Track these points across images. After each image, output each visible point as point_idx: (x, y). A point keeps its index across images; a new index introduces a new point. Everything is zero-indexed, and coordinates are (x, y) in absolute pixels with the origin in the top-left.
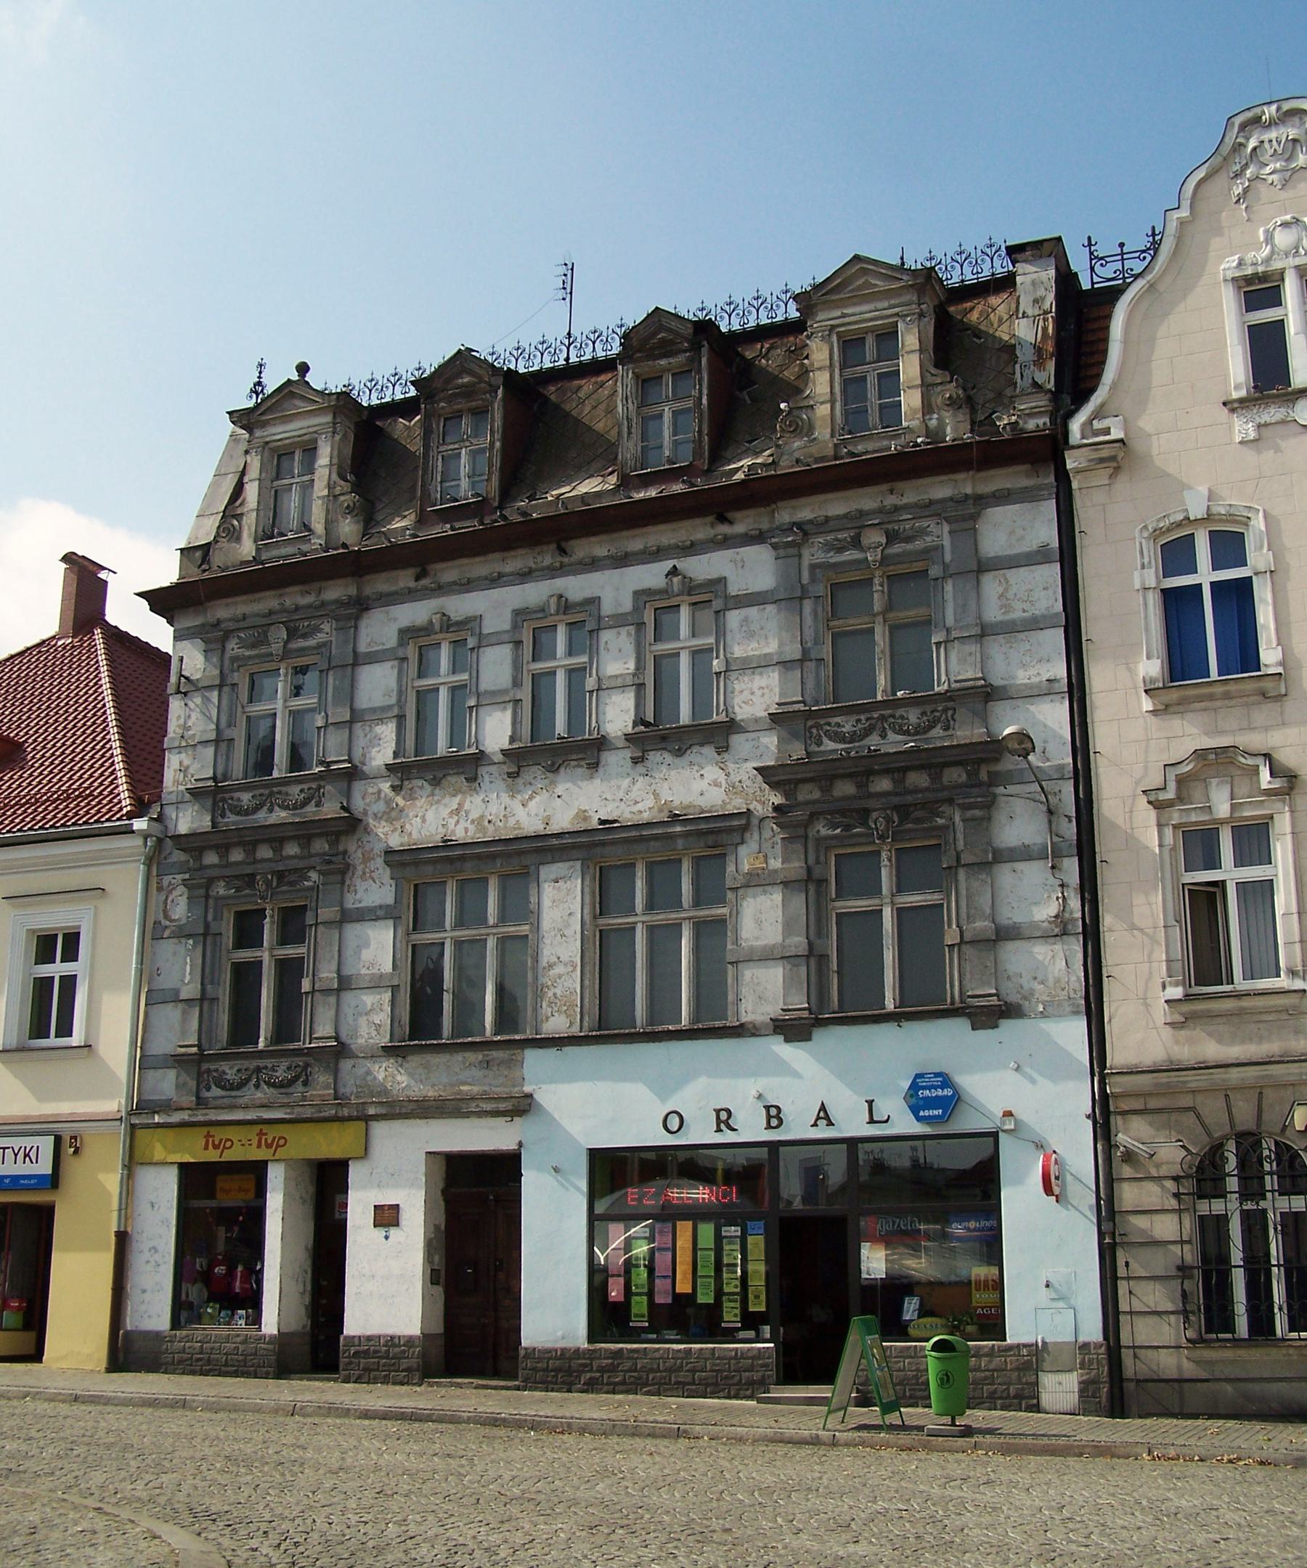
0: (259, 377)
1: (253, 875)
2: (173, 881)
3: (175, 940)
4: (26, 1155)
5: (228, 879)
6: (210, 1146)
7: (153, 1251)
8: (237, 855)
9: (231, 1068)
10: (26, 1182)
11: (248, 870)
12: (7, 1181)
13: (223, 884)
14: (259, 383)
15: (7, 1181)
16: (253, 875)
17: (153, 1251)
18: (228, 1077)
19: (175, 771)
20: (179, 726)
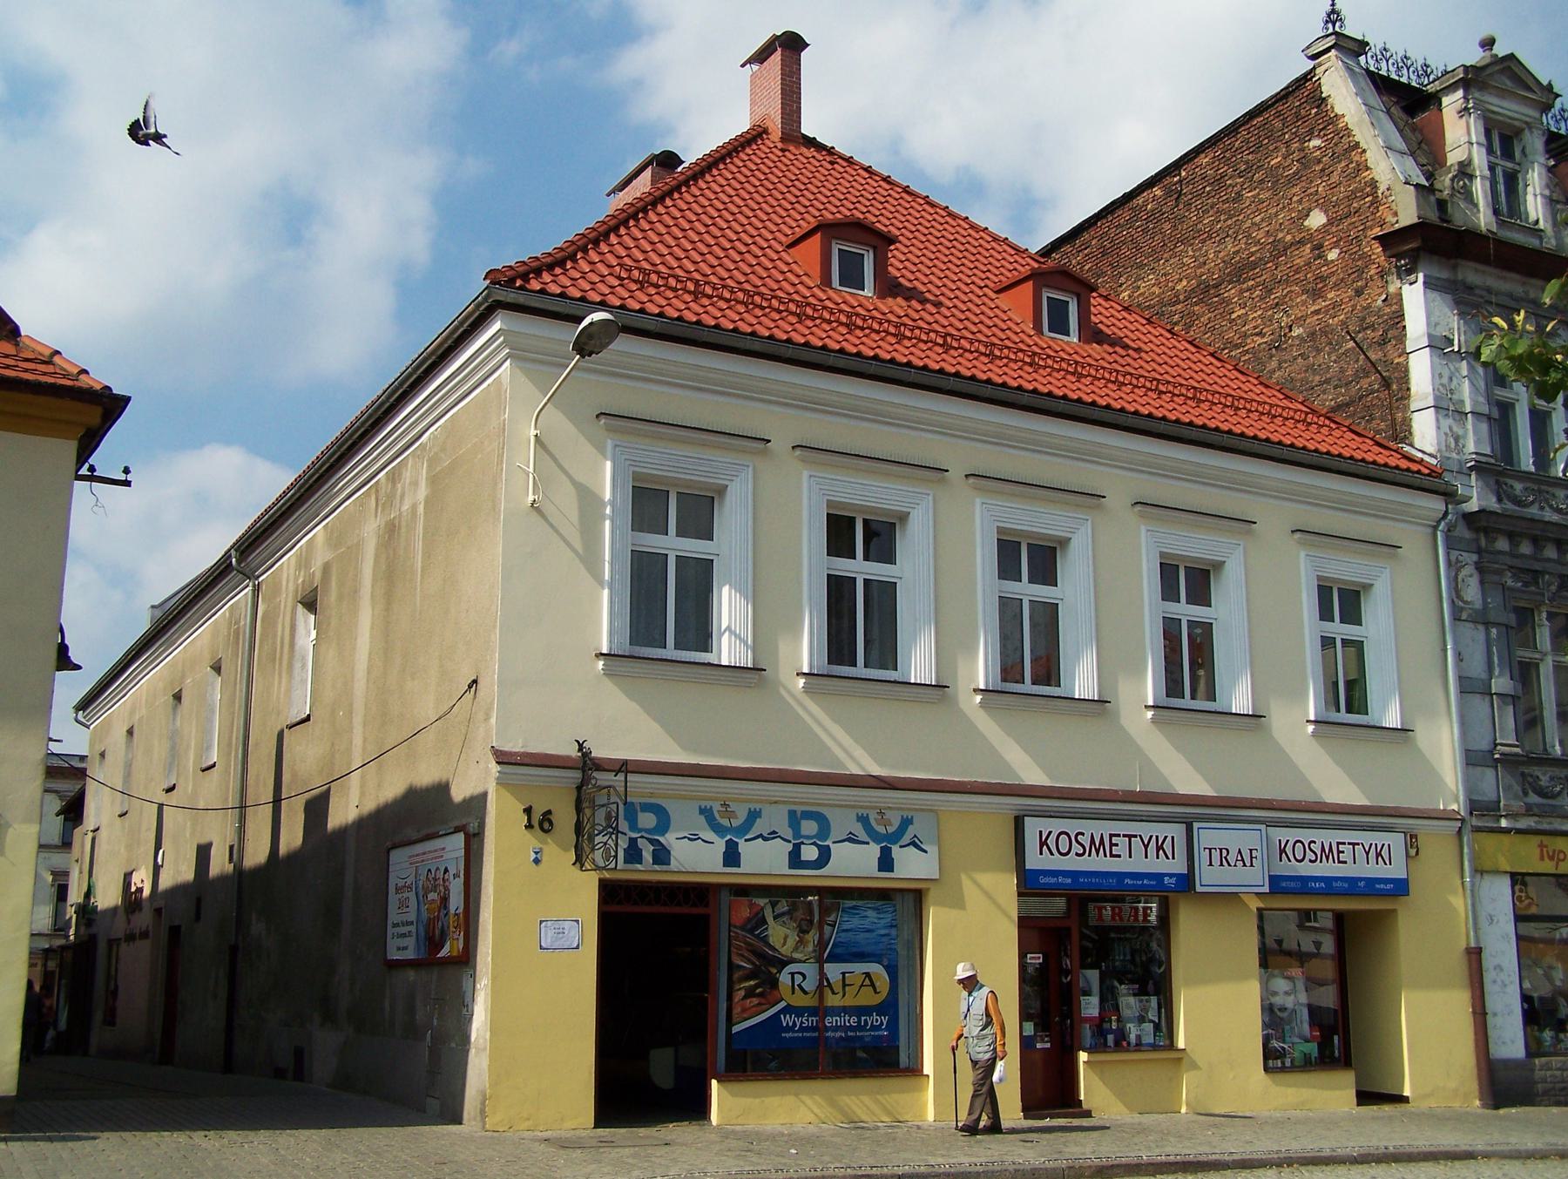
0: (1333, 5)
1: (1542, 573)
2: (1460, 557)
3: (1471, 625)
4: (1379, 855)
5: (1518, 572)
6: (1546, 858)
7: (1498, 970)
8: (1526, 548)
9: (1544, 774)
10: (1382, 886)
11: (1537, 566)
12: (1362, 884)
13: (1510, 574)
14: (1333, 11)
15: (1362, 884)
16: (1542, 573)
17: (1498, 970)
18: (1542, 783)
19: (1446, 434)
20: (1443, 385)
